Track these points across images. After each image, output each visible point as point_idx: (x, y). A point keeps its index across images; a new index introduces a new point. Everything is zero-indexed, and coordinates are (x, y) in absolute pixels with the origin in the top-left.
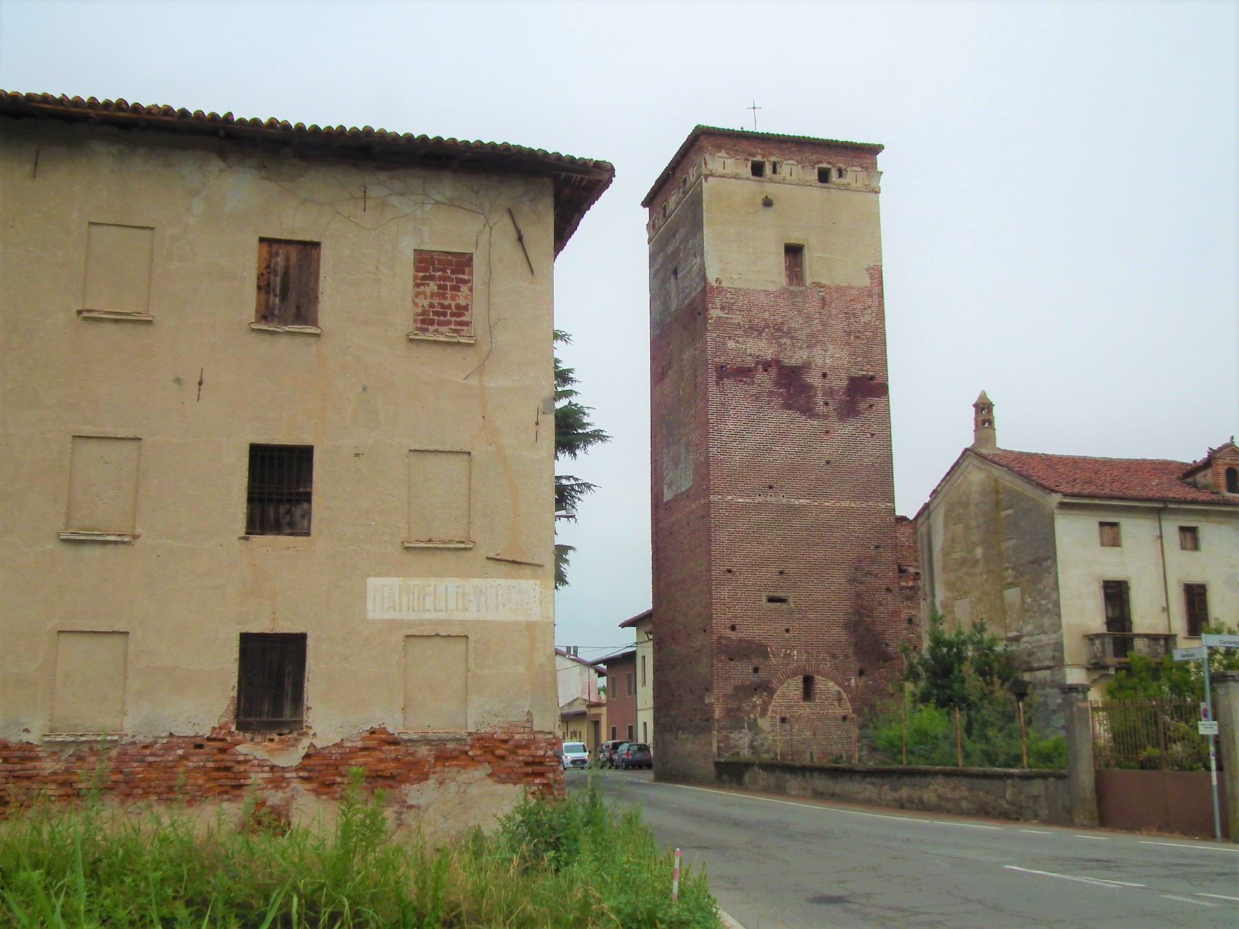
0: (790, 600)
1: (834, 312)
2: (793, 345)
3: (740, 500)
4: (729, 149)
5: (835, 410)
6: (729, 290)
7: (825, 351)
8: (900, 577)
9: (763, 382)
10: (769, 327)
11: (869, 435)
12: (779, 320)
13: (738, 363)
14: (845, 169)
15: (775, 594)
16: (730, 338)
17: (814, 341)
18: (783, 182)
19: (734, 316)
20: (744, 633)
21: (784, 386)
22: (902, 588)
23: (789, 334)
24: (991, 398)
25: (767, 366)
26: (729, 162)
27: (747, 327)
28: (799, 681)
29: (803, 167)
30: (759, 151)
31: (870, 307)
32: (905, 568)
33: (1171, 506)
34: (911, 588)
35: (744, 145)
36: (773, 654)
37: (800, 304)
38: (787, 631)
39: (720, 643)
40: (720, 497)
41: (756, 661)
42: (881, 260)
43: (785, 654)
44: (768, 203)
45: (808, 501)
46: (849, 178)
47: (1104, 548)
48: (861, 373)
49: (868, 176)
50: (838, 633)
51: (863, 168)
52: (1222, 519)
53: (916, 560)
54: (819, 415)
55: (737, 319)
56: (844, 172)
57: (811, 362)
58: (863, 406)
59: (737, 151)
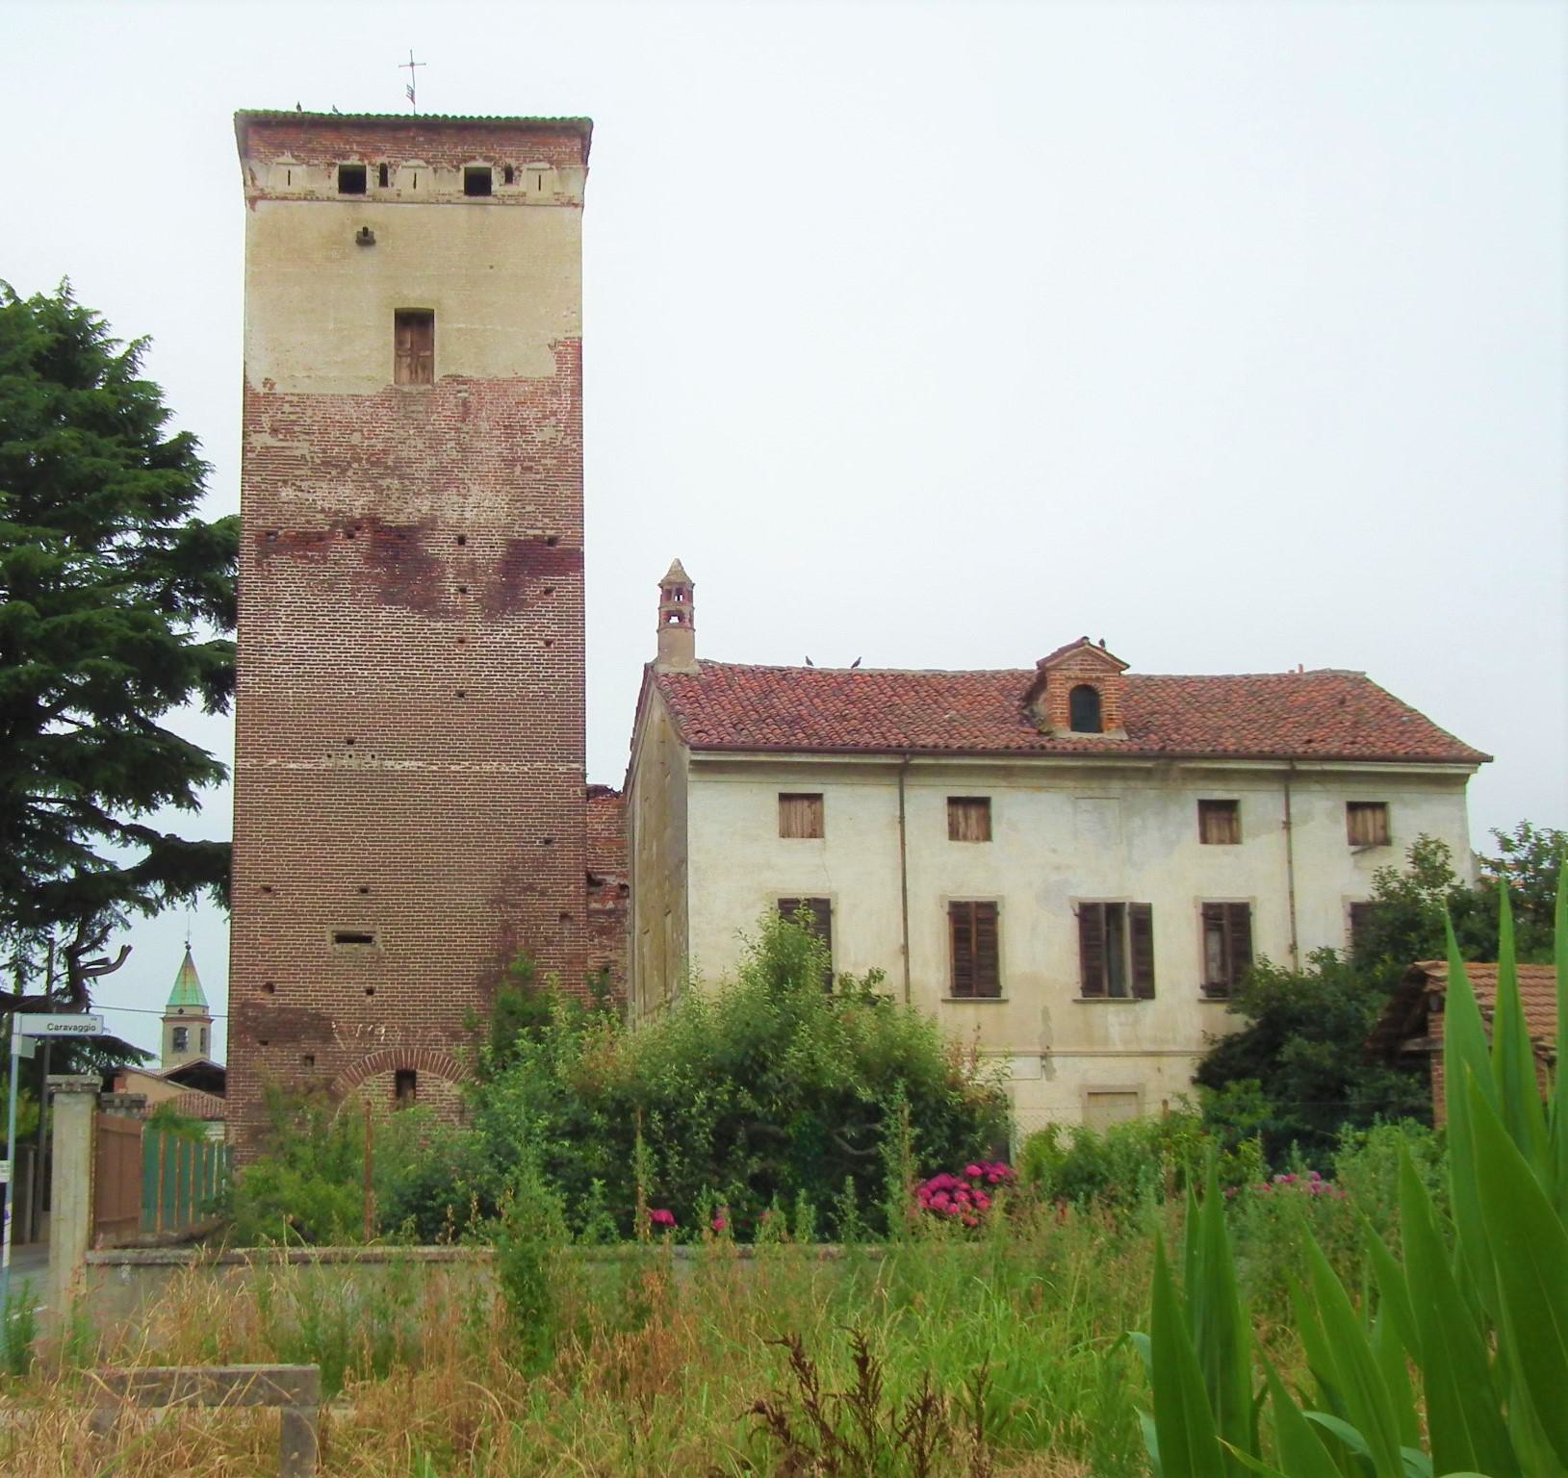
0: (378, 938)
1: (484, 426)
2: (404, 490)
3: (292, 766)
4: (298, 148)
5: (477, 600)
6: (287, 398)
7: (465, 497)
8: (589, 894)
9: (343, 558)
10: (359, 460)
11: (541, 644)
12: (380, 446)
13: (298, 525)
14: (518, 168)
15: (350, 929)
16: (285, 482)
17: (444, 480)
18: (399, 199)
19: (296, 444)
20: (288, 998)
21: (382, 562)
22: (591, 913)
23: (396, 470)
24: (692, 573)
25: (352, 528)
26: (299, 171)
27: (318, 461)
28: (388, 1077)
29: (435, 171)
30: (355, 147)
31: (554, 413)
32: (599, 877)
33: (916, 761)
34: (610, 913)
35: (328, 140)
36: (340, 1033)
37: (420, 416)
38: (370, 992)
39: (244, 1015)
40: (255, 761)
41: (308, 1045)
42: (580, 327)
43: (363, 1033)
44: (365, 239)
45: (420, 764)
46: (525, 183)
47: (787, 841)
48: (529, 532)
49: (561, 177)
50: (464, 996)
51: (551, 163)
52: (1044, 782)
53: (623, 864)
54: (447, 611)
55: (301, 448)
56: (516, 173)
57: (436, 517)
58: (531, 591)
59: (313, 150)
